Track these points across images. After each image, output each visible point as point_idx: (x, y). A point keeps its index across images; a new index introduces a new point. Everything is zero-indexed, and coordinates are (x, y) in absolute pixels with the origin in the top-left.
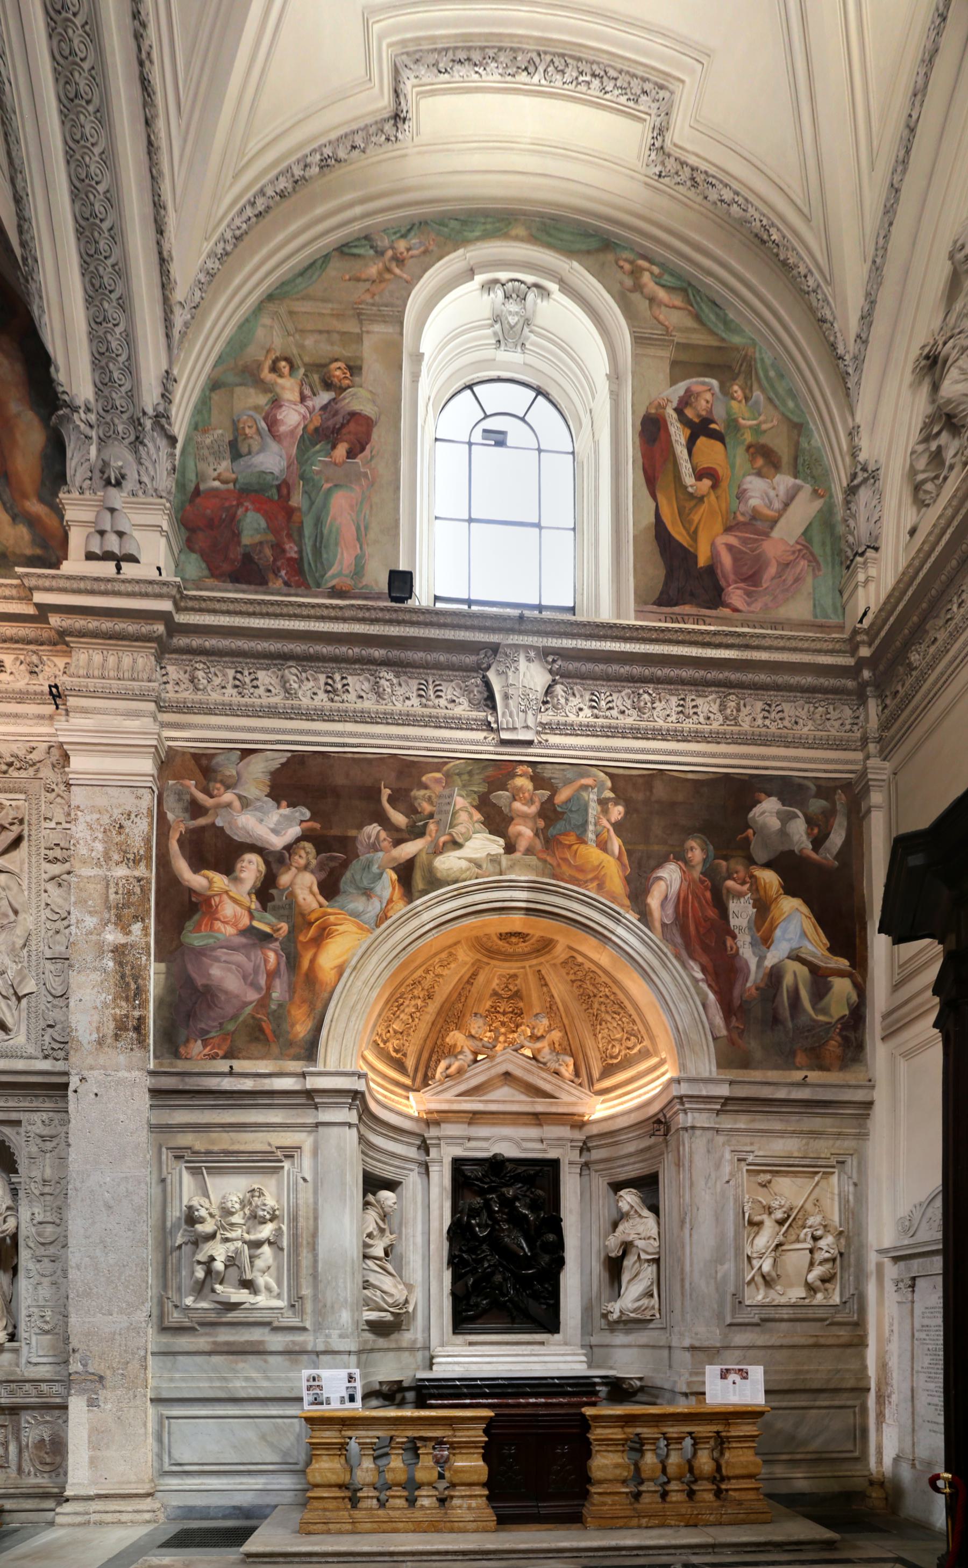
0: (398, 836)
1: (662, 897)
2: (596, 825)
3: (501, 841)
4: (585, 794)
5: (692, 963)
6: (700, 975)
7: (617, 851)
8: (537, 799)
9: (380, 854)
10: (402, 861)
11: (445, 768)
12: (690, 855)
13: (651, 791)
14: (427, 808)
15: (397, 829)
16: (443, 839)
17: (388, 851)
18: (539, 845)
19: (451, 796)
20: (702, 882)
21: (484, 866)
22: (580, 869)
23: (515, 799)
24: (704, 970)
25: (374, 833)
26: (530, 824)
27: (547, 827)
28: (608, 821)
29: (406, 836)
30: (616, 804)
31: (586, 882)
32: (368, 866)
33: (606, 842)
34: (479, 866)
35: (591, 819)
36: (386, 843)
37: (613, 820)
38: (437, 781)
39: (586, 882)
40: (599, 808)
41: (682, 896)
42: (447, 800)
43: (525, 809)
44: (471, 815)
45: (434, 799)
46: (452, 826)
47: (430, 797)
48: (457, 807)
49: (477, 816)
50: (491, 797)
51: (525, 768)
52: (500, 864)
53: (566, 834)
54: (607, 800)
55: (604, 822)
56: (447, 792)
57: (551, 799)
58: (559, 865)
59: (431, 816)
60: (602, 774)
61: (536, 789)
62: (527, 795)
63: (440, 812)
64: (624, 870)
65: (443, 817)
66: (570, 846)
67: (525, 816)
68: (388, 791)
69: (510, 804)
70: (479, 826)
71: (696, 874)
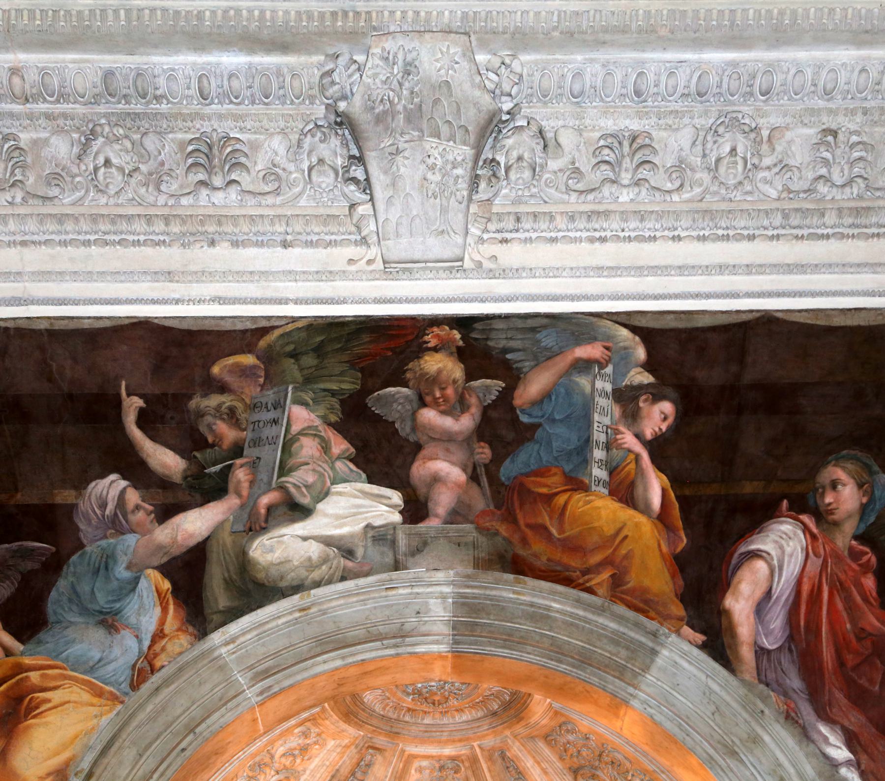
0: (170, 498)
1: (759, 593)
2: (608, 447)
3: (396, 497)
4: (584, 382)
5: (824, 729)
6: (841, 753)
7: (656, 501)
8: (473, 400)
9: (131, 539)
10: (176, 552)
11: (263, 343)
12: (828, 499)
13: (742, 362)
14: (228, 434)
15: (164, 483)
16: (265, 500)
17: (150, 532)
18: (479, 502)
19: (279, 405)
20: (854, 555)
21: (360, 552)
22: (573, 547)
23: (423, 404)
24: (851, 740)
25: (114, 493)
26: (460, 455)
27: (497, 460)
28: (638, 436)
29: (182, 497)
30: (657, 398)
31: (586, 572)
32: (107, 562)
33: (632, 485)
34: (348, 553)
35: (599, 436)
36: (141, 515)
37: (649, 434)
38: (245, 372)
39: (586, 572)
40: (617, 411)
41: (806, 588)
42: (271, 415)
43: (448, 423)
44: (325, 447)
45: (243, 416)
46: (284, 470)
47: (232, 411)
48: (295, 429)
49: (340, 445)
50: (370, 401)
51: (444, 331)
52: (393, 543)
53: (542, 472)
54: (637, 390)
55: (629, 440)
56: (270, 395)
57: (506, 396)
58: (524, 541)
59: (237, 451)
60: (624, 332)
61: (470, 376)
62: (450, 391)
63: (256, 442)
64: (672, 543)
65: (265, 452)
66: (549, 498)
67: (447, 438)
68: (138, 402)
69: (414, 413)
70: (343, 467)
71: (844, 539)
